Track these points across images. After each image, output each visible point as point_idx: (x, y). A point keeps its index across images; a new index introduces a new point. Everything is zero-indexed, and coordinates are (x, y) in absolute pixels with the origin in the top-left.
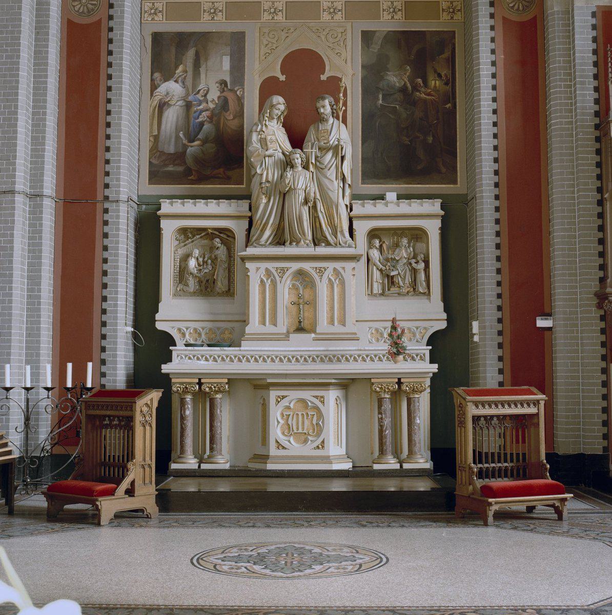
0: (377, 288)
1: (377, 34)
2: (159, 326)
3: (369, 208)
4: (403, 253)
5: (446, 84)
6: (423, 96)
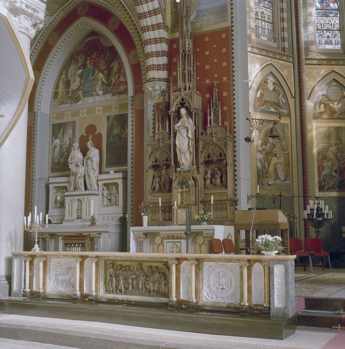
1: (111, 117)
6: (124, 136)
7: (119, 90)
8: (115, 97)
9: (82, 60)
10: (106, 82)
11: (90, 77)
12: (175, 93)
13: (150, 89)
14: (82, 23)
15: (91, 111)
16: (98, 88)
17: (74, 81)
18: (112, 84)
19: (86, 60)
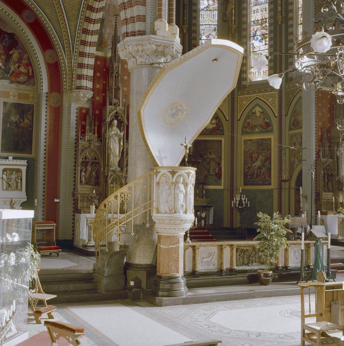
0: (5, 188)
4: (14, 176)
5: (30, 122)
6: (22, 125)
7: (18, 80)
8: (14, 86)
12: (110, 106)
13: (82, 95)
18: (11, 71)
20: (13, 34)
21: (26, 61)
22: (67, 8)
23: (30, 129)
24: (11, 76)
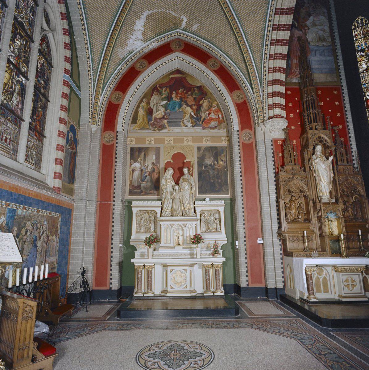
2: (131, 243)
3: (201, 203)
5: (225, 163)
6: (217, 167)
7: (210, 125)
9: (166, 92)
10: (195, 116)
11: (177, 109)
14: (176, 58)
15: (178, 139)
16: (186, 121)
17: (157, 110)
18: (202, 119)
19: (171, 93)
20: (201, 86)
21: (215, 108)
22: (250, 40)
23: (225, 170)
24: (202, 123)
